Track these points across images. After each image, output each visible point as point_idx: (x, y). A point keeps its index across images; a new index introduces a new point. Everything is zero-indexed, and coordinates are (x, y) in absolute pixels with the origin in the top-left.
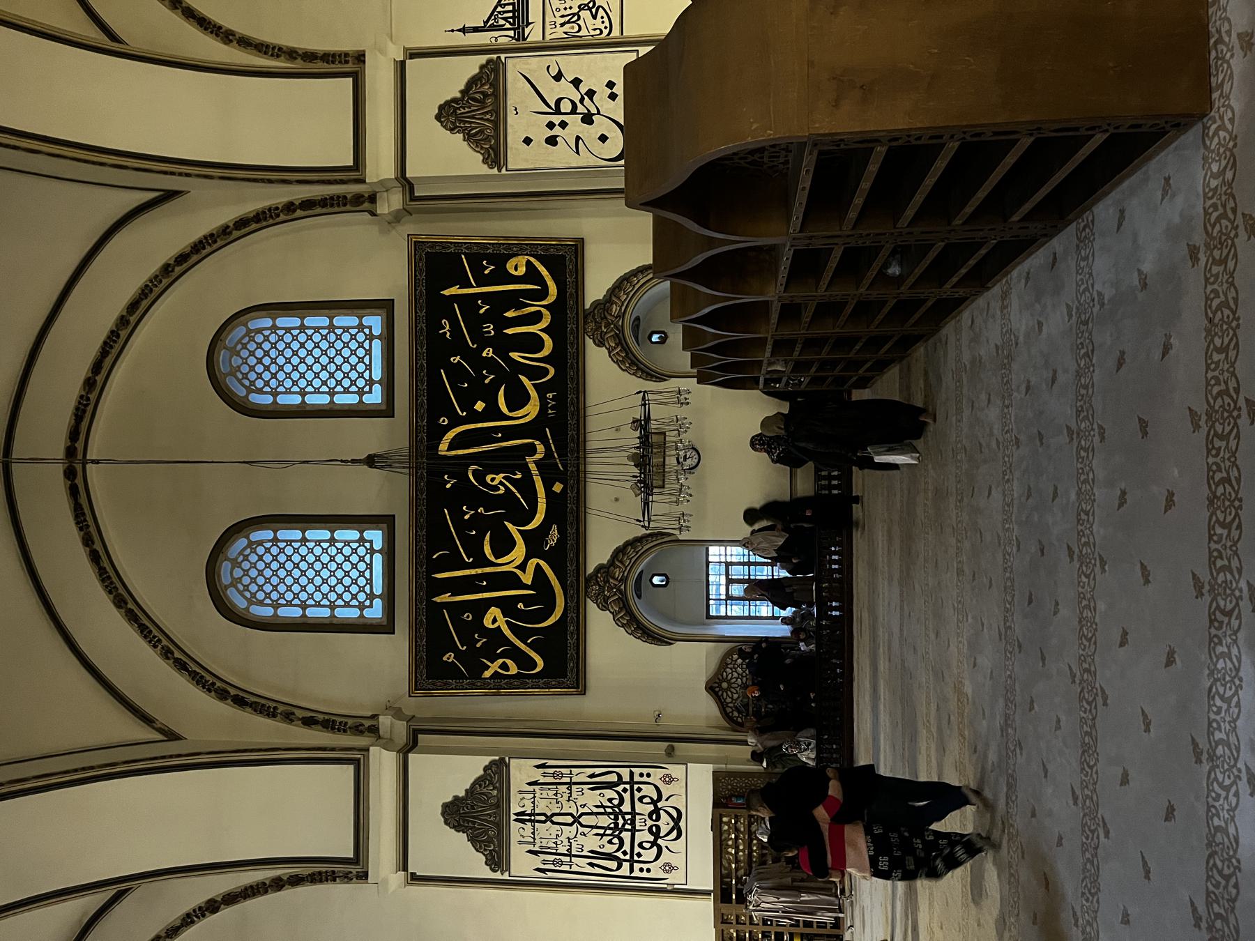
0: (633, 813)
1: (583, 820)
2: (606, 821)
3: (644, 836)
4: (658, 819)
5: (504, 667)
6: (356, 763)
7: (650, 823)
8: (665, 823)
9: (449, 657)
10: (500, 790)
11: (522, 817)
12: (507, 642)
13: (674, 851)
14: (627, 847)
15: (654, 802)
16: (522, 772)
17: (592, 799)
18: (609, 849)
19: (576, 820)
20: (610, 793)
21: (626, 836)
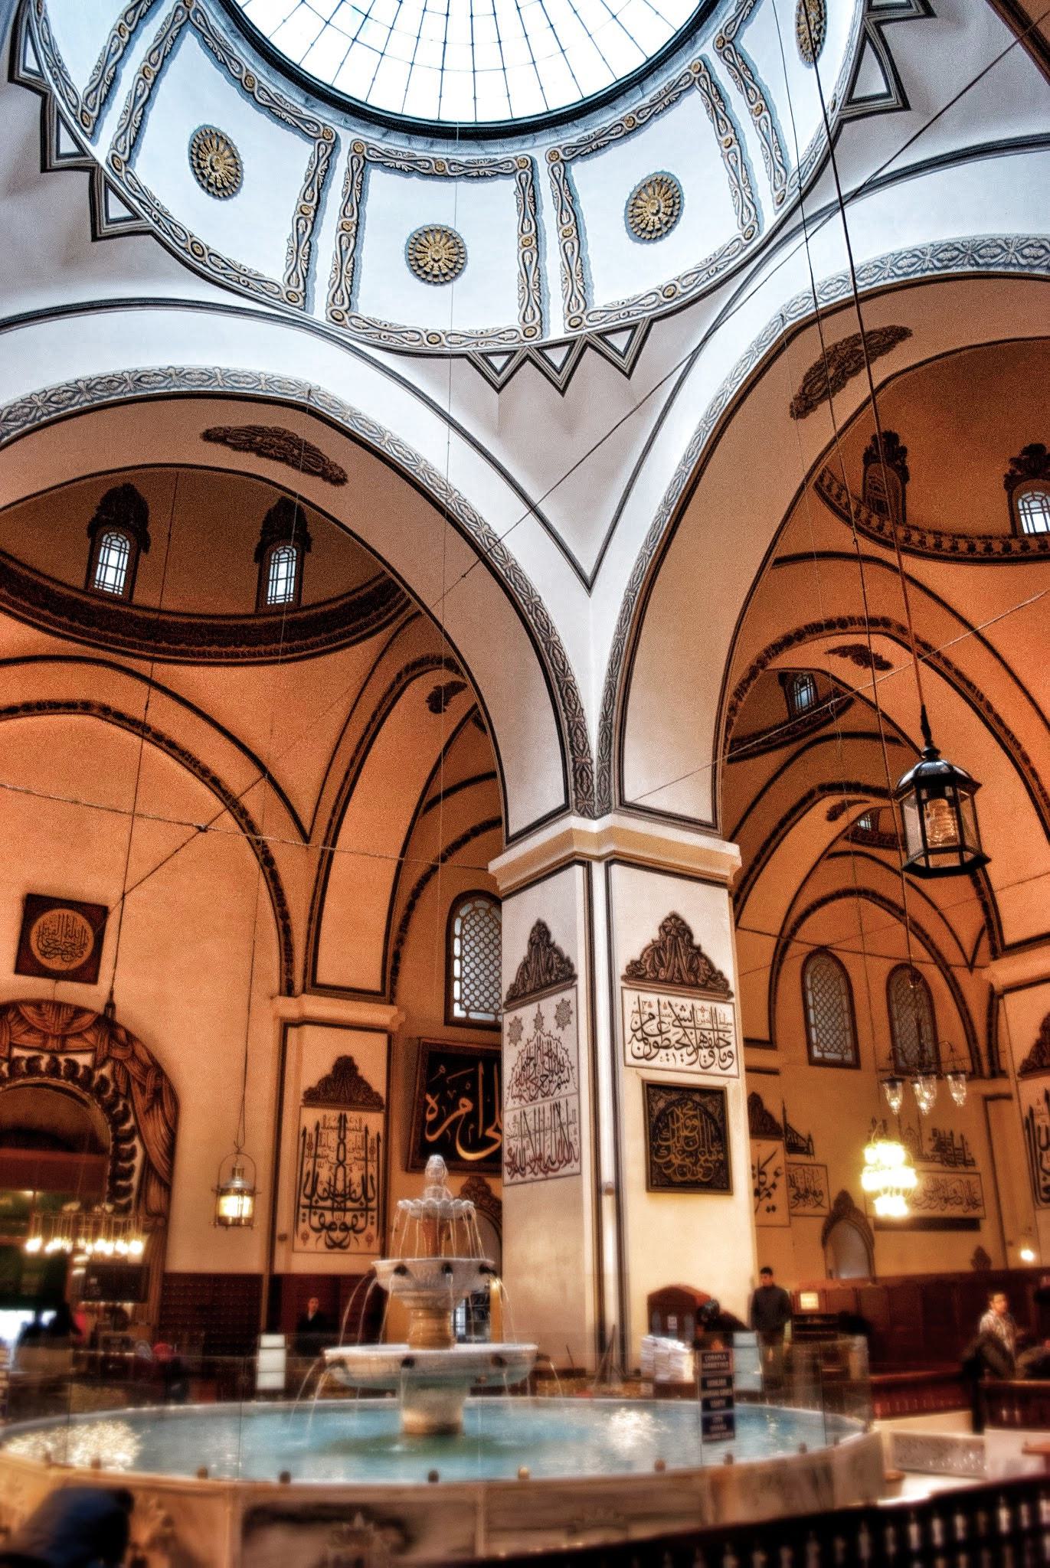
0: (345, 1210)
1: (341, 1170)
2: (340, 1186)
3: (328, 1217)
4: (342, 1230)
5: (432, 1111)
6: (382, 993)
7: (338, 1223)
8: (337, 1235)
9: (442, 1069)
10: (363, 1103)
11: (343, 1120)
12: (449, 1113)
13: (317, 1242)
14: (321, 1203)
15: (353, 1227)
16: (374, 1121)
17: (356, 1176)
18: (320, 1190)
19: (341, 1163)
20: (359, 1191)
21: (329, 1203)
